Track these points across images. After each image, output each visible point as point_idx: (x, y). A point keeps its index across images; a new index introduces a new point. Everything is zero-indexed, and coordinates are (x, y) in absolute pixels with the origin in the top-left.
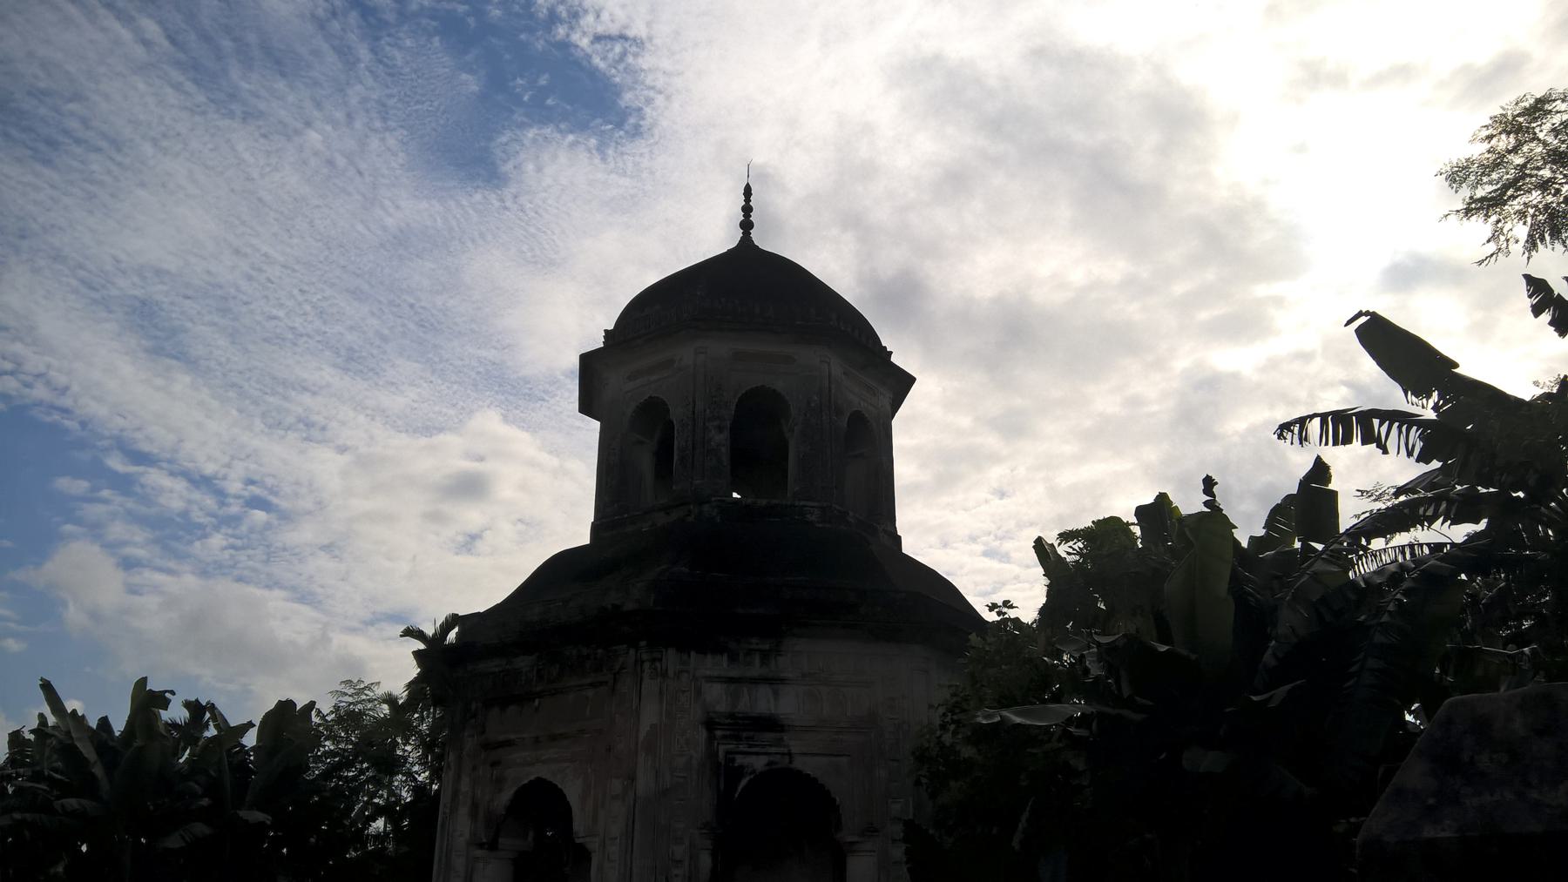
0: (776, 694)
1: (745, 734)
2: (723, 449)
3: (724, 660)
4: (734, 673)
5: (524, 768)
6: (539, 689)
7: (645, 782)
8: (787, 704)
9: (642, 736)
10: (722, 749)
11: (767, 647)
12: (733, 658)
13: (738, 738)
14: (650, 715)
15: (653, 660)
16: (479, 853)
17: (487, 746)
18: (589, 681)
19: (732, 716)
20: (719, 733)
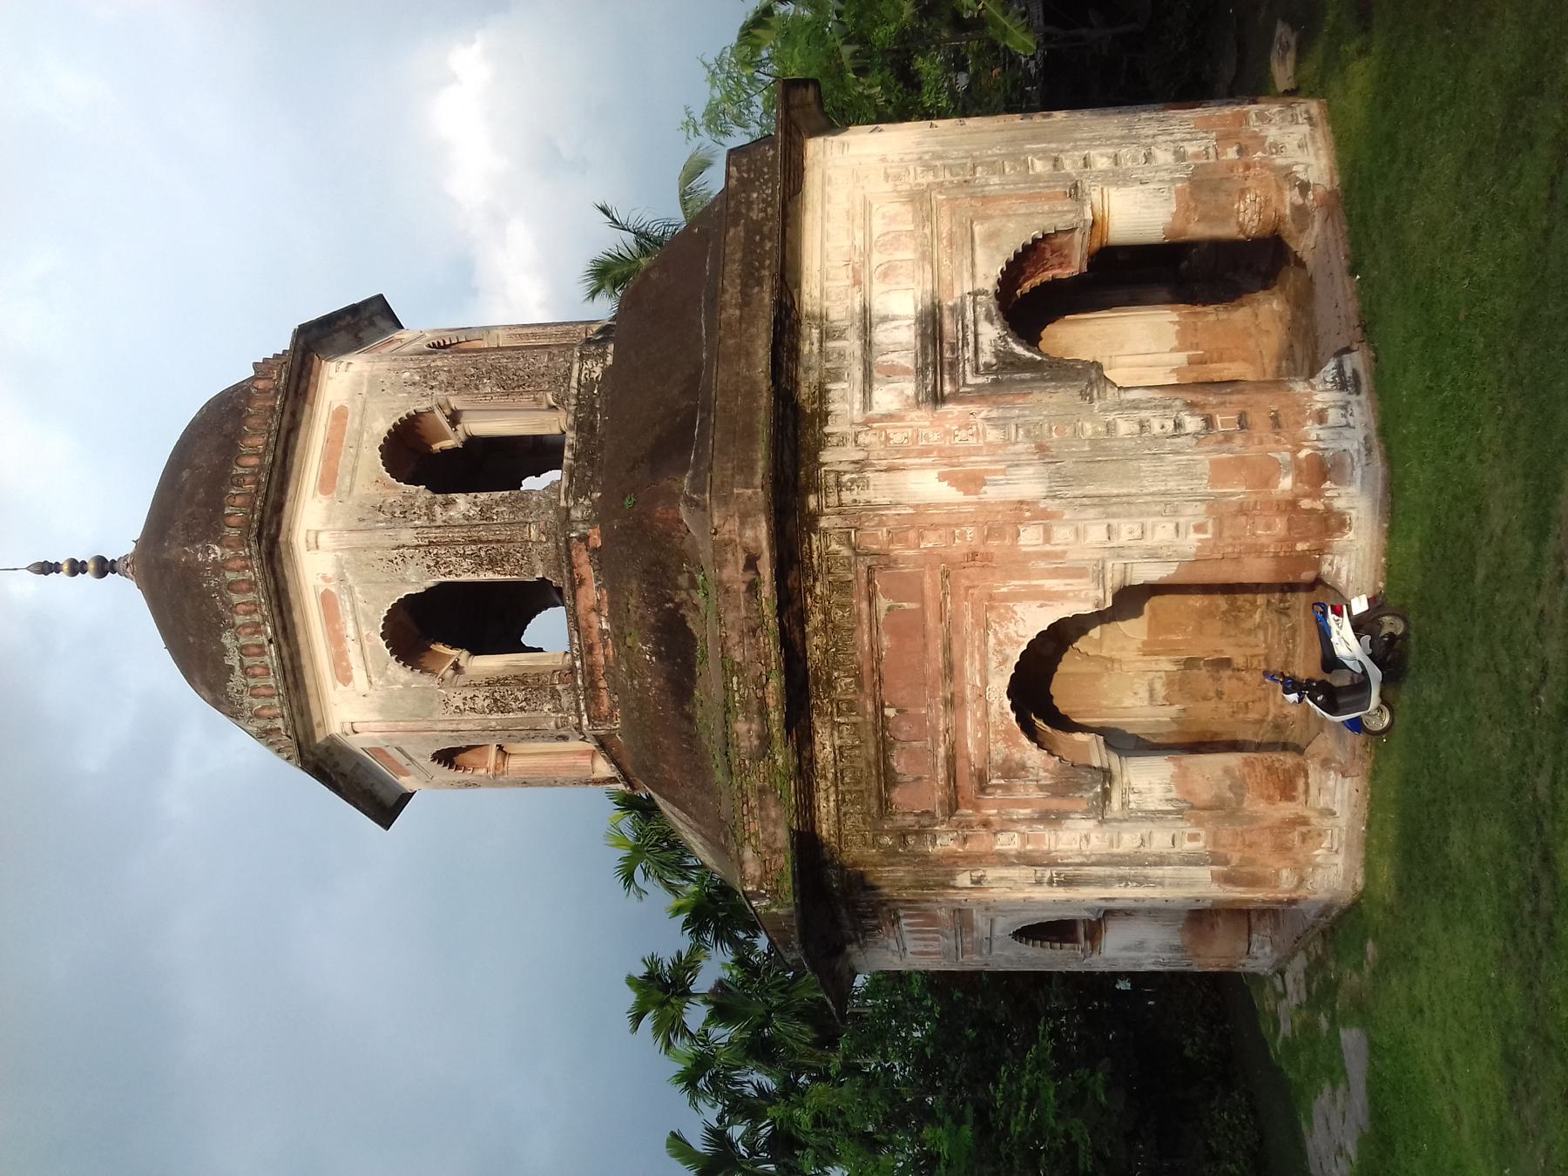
0: (885, 319)
1: (947, 355)
2: (483, 496)
3: (836, 388)
4: (858, 373)
6: (870, 708)
7: (1028, 484)
8: (899, 306)
11: (815, 333)
12: (837, 376)
13: (953, 365)
14: (925, 486)
15: (839, 484)
16: (1116, 803)
17: (952, 806)
18: (864, 605)
19: (921, 372)
20: (948, 388)
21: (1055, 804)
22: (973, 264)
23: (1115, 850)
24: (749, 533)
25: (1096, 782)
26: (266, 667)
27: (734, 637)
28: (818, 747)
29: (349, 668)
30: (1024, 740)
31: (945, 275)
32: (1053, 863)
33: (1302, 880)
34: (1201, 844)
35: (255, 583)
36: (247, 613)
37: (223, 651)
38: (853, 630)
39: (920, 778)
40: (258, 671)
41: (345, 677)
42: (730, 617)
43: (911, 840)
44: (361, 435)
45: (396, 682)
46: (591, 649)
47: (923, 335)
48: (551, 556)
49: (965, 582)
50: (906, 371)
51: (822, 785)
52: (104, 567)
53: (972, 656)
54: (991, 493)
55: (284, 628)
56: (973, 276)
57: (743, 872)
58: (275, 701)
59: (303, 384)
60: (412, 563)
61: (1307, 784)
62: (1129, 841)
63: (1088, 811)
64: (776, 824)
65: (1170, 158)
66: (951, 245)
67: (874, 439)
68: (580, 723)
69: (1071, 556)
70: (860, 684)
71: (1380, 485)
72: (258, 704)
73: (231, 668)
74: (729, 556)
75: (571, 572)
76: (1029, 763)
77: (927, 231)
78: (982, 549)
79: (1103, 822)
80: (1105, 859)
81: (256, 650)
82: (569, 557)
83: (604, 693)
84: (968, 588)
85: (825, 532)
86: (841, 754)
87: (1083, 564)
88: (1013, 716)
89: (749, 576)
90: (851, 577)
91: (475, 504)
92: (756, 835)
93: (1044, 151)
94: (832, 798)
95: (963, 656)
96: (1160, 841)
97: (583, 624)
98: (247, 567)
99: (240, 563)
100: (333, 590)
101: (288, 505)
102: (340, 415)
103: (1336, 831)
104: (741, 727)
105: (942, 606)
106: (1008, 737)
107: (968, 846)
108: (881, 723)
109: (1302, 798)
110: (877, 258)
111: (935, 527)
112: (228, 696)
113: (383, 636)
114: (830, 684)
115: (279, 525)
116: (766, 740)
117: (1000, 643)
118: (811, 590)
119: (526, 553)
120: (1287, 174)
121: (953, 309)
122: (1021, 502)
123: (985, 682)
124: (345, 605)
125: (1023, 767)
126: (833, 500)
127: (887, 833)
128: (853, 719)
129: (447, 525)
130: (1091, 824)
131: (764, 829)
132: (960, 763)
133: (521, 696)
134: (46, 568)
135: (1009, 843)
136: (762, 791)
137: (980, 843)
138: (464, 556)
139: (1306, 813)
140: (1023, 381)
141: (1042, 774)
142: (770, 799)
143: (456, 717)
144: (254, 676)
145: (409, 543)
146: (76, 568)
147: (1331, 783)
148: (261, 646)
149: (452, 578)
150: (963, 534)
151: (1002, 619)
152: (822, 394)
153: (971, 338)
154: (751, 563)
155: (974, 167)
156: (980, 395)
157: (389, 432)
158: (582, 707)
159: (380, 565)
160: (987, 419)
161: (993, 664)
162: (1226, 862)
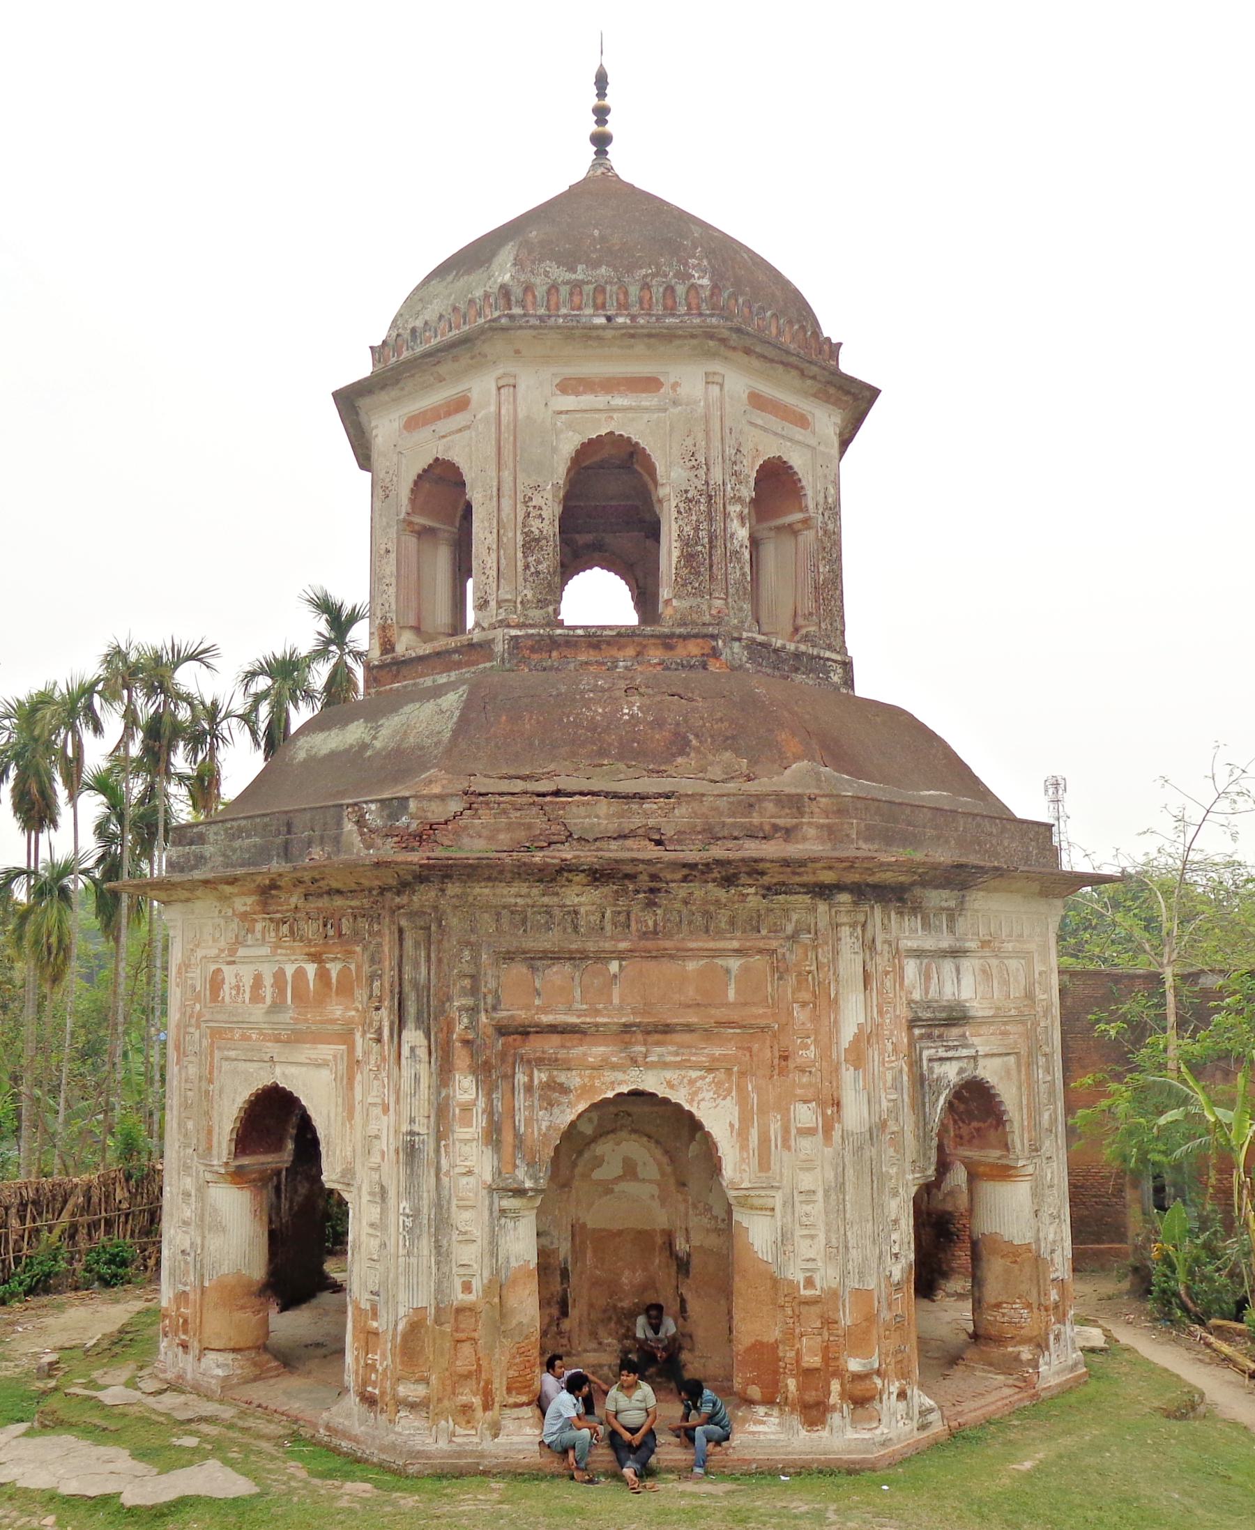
0: (958, 970)
1: (936, 1032)
6: (623, 945)
8: (964, 986)
9: (845, 1044)
10: (926, 1054)
11: (952, 904)
12: (926, 925)
13: (929, 1036)
16: (506, 1203)
18: (735, 944)
19: (928, 1005)
20: (917, 1032)
21: (508, 1137)
22: (993, 1055)
23: (454, 1202)
24: (812, 832)
25: (536, 1180)
26: (580, 308)
28: (577, 889)
29: (577, 394)
31: (984, 1030)
32: (441, 1135)
33: (413, 1406)
34: (461, 1296)
35: (673, 315)
36: (641, 301)
37: (596, 265)
38: (707, 931)
40: (576, 299)
41: (565, 387)
44: (791, 440)
47: (950, 1008)
48: (695, 616)
49: (756, 1047)
50: (927, 993)
51: (535, 891)
52: (601, 141)
53: (677, 1054)
54: (848, 1074)
55: (633, 336)
56: (986, 1056)
58: (542, 311)
59: (832, 390)
61: (522, 1405)
63: (500, 1173)
65: (1051, 1237)
66: (1002, 1033)
67: (886, 959)
68: (509, 626)
69: (785, 1154)
70: (644, 935)
72: (540, 291)
73: (572, 269)
74: (788, 811)
75: (680, 636)
76: (556, 1110)
77: (1013, 1012)
78: (791, 1065)
79: (491, 1190)
81: (599, 301)
82: (696, 636)
84: (750, 1050)
86: (569, 913)
87: (775, 1166)
88: (610, 1095)
89: (767, 828)
90: (764, 932)
91: (741, 546)
92: (476, 816)
93: (1056, 1119)
94: (519, 900)
95: (672, 1043)
98: (690, 308)
99: (694, 302)
100: (662, 391)
101: (746, 358)
102: (802, 421)
103: (476, 1440)
104: (603, 806)
105: (730, 1024)
106: (585, 1090)
107: (458, 1044)
108: (601, 958)
109: (511, 1401)
110: (994, 962)
111: (815, 1018)
112: (541, 261)
113: (611, 433)
114: (651, 904)
115: (734, 349)
117: (692, 1082)
119: (698, 593)
120: (1041, 1345)
121: (964, 1035)
122: (838, 1104)
123: (650, 1066)
124: (647, 400)
126: (844, 919)
127: (475, 959)
128: (608, 927)
129: (726, 515)
130: (488, 1178)
132: (556, 1039)
134: (601, 81)
137: (461, 1058)
138: (697, 529)
139: (497, 1406)
140: (924, 1105)
143: (520, 497)
144: (571, 294)
145: (711, 475)
146: (601, 113)
147: (528, 1430)
148: (603, 306)
150: (807, 1047)
151: (719, 1084)
152: (916, 909)
153: (950, 1054)
155: (1046, 1055)
156: (915, 1063)
157: (791, 468)
158: (531, 631)
159: (689, 442)
160: (901, 1071)
161: (669, 1074)
162: (437, 1321)
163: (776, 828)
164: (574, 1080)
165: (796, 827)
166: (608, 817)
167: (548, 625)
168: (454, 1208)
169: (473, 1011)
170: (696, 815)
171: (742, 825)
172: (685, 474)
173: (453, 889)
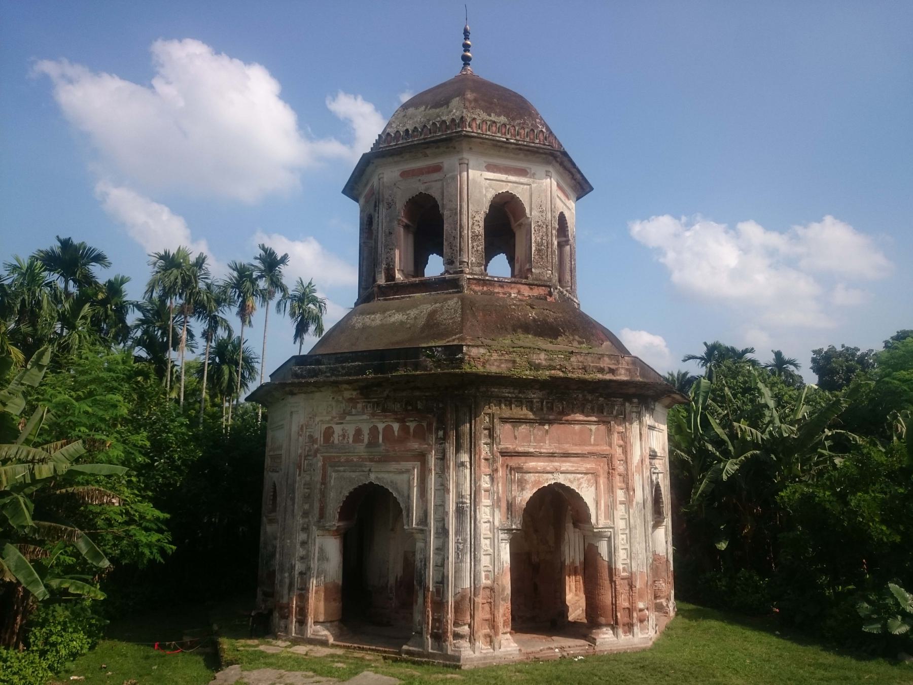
5: (542, 474)
6: (551, 417)
24: (623, 371)
27: (581, 359)
30: (535, 490)
37: (499, 115)
39: (516, 438)
40: (494, 128)
42: (589, 359)
43: (486, 432)
45: (487, 191)
46: (502, 287)
51: (516, 391)
55: (520, 149)
57: (473, 346)
60: (540, 215)
62: (485, 544)
64: (498, 366)
71: (643, 646)
75: (536, 285)
76: (524, 492)
80: (478, 531)
83: (481, 288)
85: (623, 405)
88: (546, 485)
89: (606, 369)
96: (485, 561)
97: (513, 285)
104: (543, 356)
106: (537, 482)
116: (538, 367)
117: (578, 479)
118: (601, 396)
125: (523, 490)
126: (635, 410)
128: (545, 409)
131: (496, 360)
133: (479, 248)
135: (485, 482)
136: (514, 362)
137: (485, 468)
138: (542, 239)
141: (520, 499)
142: (510, 365)
149: (533, 231)
151: (589, 481)
154: (612, 371)
159: (539, 200)
161: (569, 476)
163: (609, 368)
164: (531, 477)
165: (617, 369)
166: (546, 360)
167: (482, 274)
168: (482, 539)
169: (490, 445)
170: (579, 362)
171: (596, 367)
172: (537, 214)
173: (483, 389)
